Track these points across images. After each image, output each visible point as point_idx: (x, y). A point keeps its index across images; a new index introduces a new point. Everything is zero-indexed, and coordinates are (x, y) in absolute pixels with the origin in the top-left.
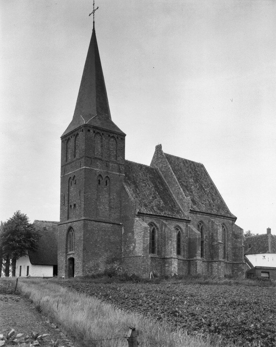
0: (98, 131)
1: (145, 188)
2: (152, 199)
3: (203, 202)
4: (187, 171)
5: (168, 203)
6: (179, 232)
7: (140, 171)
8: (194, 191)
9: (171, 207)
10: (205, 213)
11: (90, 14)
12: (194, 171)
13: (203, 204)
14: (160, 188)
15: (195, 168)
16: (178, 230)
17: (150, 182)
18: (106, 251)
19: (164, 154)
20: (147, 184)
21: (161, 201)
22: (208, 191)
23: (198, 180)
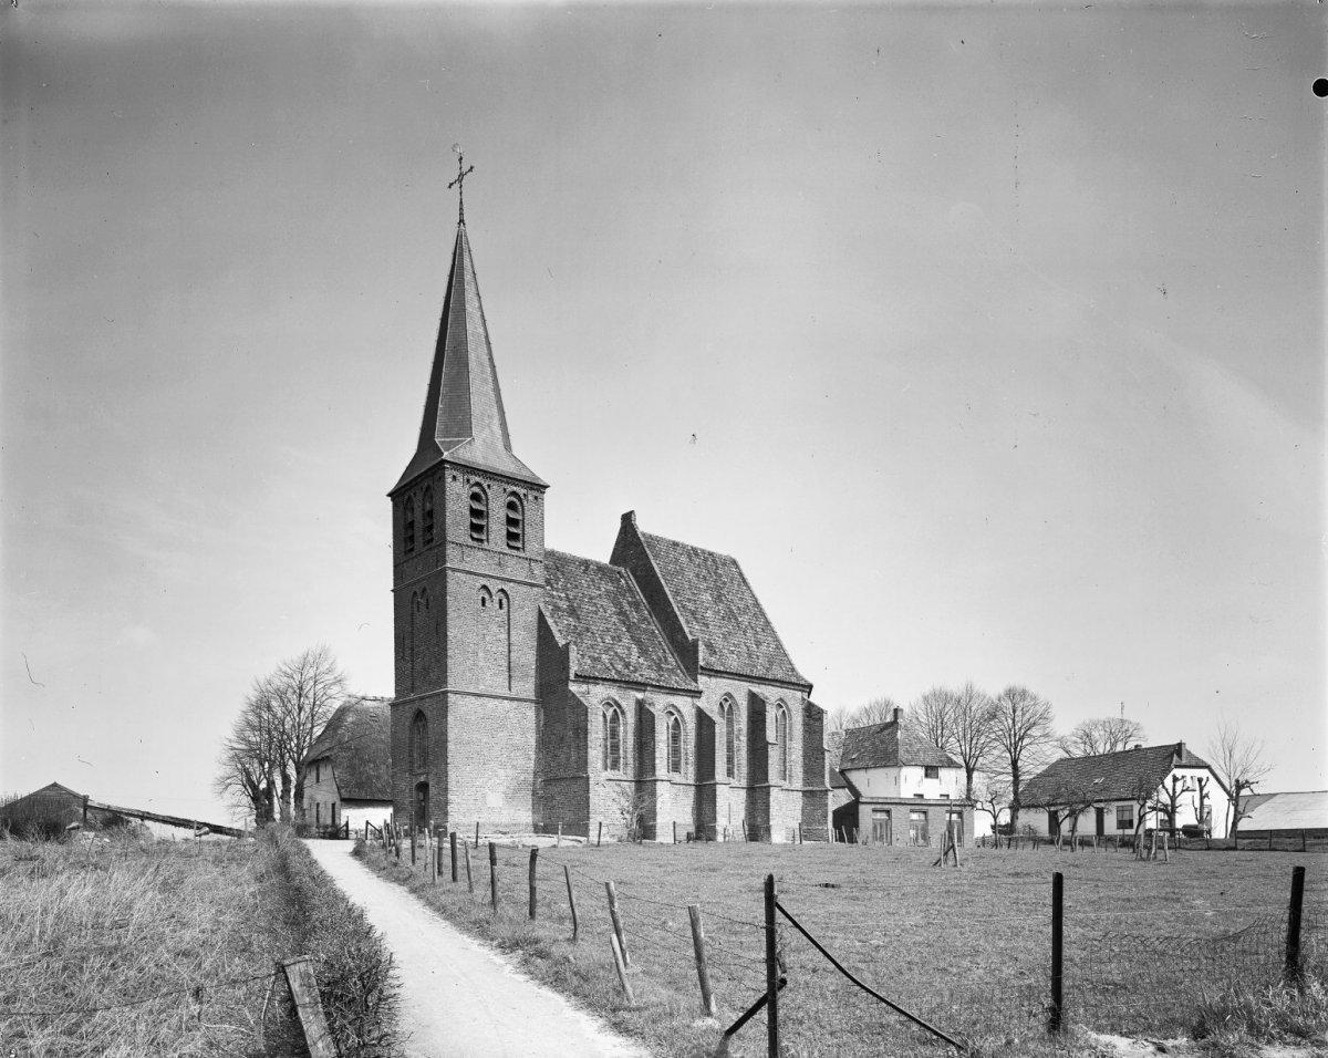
0: (477, 479)
4: (697, 576)
6: (676, 719)
10: (736, 674)
11: (451, 184)
17: (605, 602)
18: (503, 765)
19: (640, 536)
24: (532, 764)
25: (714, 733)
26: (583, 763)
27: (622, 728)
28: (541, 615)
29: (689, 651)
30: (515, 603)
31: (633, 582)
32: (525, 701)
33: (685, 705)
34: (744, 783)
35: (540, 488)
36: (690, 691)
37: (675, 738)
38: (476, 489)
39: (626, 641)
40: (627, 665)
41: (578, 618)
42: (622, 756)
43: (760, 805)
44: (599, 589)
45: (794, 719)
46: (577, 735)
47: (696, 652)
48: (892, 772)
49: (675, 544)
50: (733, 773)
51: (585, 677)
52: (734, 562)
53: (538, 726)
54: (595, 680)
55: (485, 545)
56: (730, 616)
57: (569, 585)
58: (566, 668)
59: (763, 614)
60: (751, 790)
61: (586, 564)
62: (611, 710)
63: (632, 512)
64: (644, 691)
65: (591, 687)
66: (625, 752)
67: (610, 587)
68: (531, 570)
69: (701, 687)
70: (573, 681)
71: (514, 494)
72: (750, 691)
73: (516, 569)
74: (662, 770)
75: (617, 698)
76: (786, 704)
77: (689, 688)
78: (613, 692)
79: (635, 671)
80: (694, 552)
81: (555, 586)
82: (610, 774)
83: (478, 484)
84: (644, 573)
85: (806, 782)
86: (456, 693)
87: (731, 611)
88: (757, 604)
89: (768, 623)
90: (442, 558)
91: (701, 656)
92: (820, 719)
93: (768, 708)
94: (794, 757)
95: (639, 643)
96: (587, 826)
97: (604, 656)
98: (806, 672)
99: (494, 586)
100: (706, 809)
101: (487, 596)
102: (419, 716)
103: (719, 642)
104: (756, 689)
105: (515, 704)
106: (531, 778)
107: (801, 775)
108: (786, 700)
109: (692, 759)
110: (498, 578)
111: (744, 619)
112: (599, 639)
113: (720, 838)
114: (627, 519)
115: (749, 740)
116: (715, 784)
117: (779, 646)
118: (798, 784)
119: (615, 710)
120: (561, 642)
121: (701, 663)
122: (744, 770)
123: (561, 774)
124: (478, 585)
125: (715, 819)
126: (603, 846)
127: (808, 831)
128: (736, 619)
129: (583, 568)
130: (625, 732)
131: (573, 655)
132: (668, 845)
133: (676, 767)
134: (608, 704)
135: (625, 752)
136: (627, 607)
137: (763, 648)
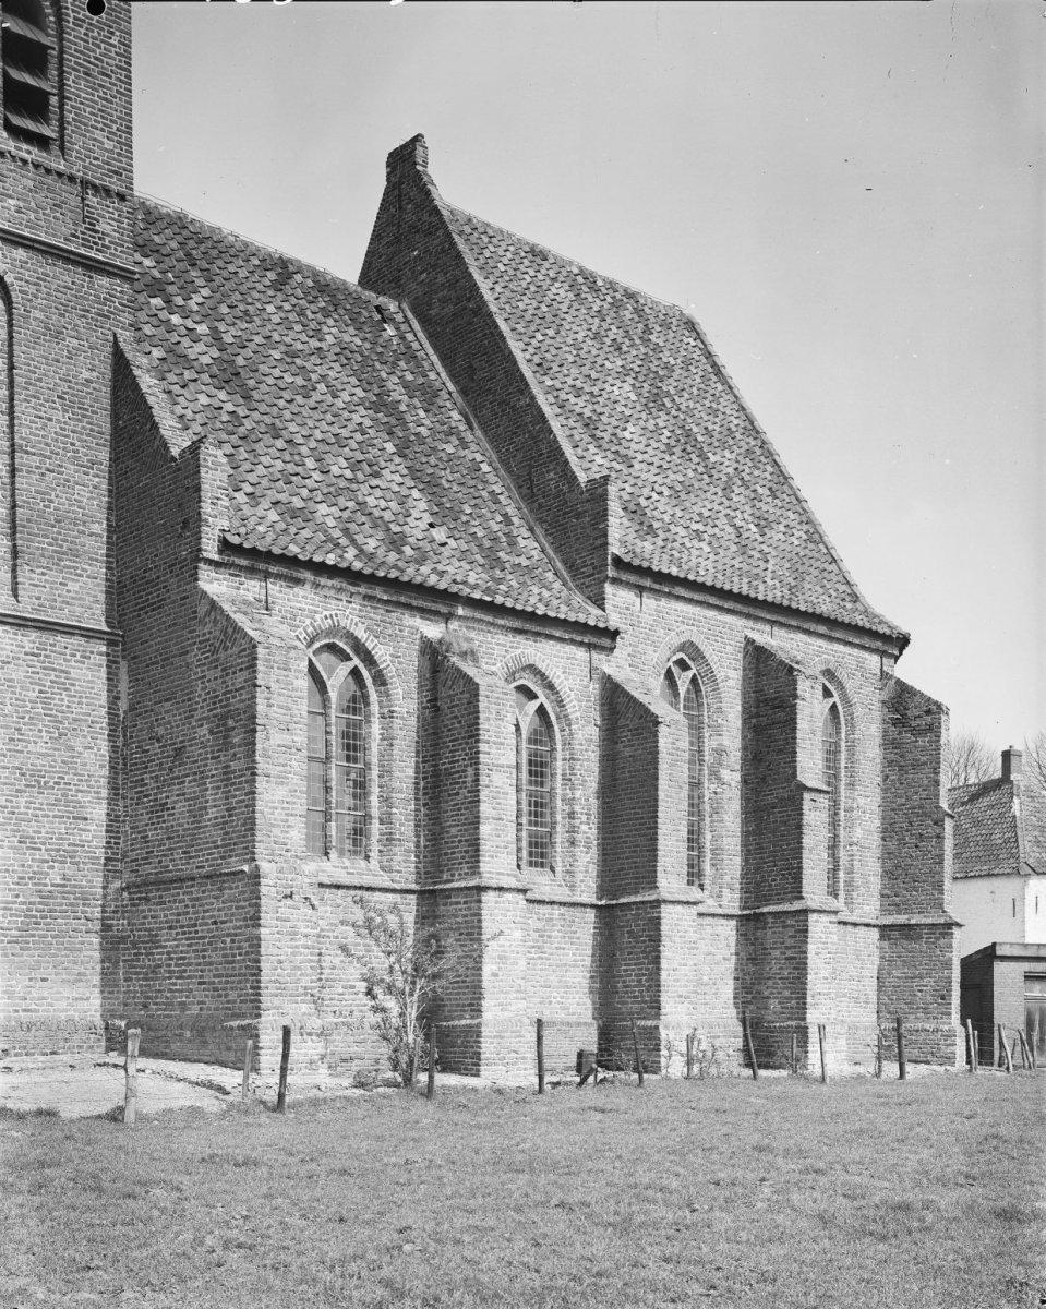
1: (299, 400)
2: (348, 473)
3: (695, 526)
5: (464, 518)
6: (541, 711)
7: (271, 293)
8: (640, 457)
9: (487, 543)
12: (638, 342)
13: (698, 535)
14: (408, 418)
15: (647, 330)
16: (535, 697)
20: (314, 377)
21: (416, 494)
22: (730, 470)
23: (668, 394)
24: (94, 835)
25: (654, 752)
26: (242, 828)
27: (376, 728)
28: (121, 368)
29: (578, 515)
31: (419, 338)
32: (67, 630)
33: (566, 665)
34: (731, 902)
36: (582, 628)
37: (538, 769)
39: (394, 476)
40: (396, 542)
41: (247, 397)
42: (375, 812)
43: (776, 963)
44: (318, 334)
45: (861, 727)
46: (222, 734)
47: (602, 515)
48: (1006, 887)
49: (538, 254)
50: (700, 874)
51: (253, 553)
52: (691, 326)
53: (112, 714)
54: (291, 567)
56: (686, 445)
57: (224, 309)
58: (191, 523)
59: (770, 454)
60: (751, 923)
61: (283, 270)
62: (343, 669)
63: (417, 139)
64: (448, 617)
65: (275, 588)
66: (386, 800)
67: (351, 337)
69: (614, 621)
70: (216, 564)
72: (749, 641)
74: (499, 856)
75: (361, 633)
76: (841, 686)
77: (582, 618)
78: (348, 613)
79: (421, 560)
80: (585, 283)
81: (179, 301)
82: (337, 868)
84: (449, 309)
85: (890, 901)
87: (688, 434)
88: (752, 429)
89: (782, 477)
91: (614, 534)
92: (933, 730)
93: (803, 687)
94: (858, 833)
95: (431, 487)
96: (252, 1033)
97: (323, 509)
98: (886, 605)
100: (629, 973)
103: (661, 509)
104: (765, 636)
105: (31, 639)
106: (93, 880)
107: (876, 883)
108: (842, 675)
109: (589, 830)
111: (724, 460)
112: (310, 463)
113: (675, 1067)
114: (405, 165)
115: (745, 781)
116: (657, 903)
117: (815, 536)
118: (869, 907)
119: (355, 673)
120: (178, 442)
121: (615, 548)
122: (733, 865)
123: (178, 865)
125: (655, 1007)
126: (292, 1107)
127: (896, 1044)
128: (703, 456)
129: (271, 275)
130: (388, 739)
131: (214, 476)
132: (518, 1098)
133: (539, 853)
134: (332, 648)
135: (386, 800)
136: (398, 394)
137: (776, 534)
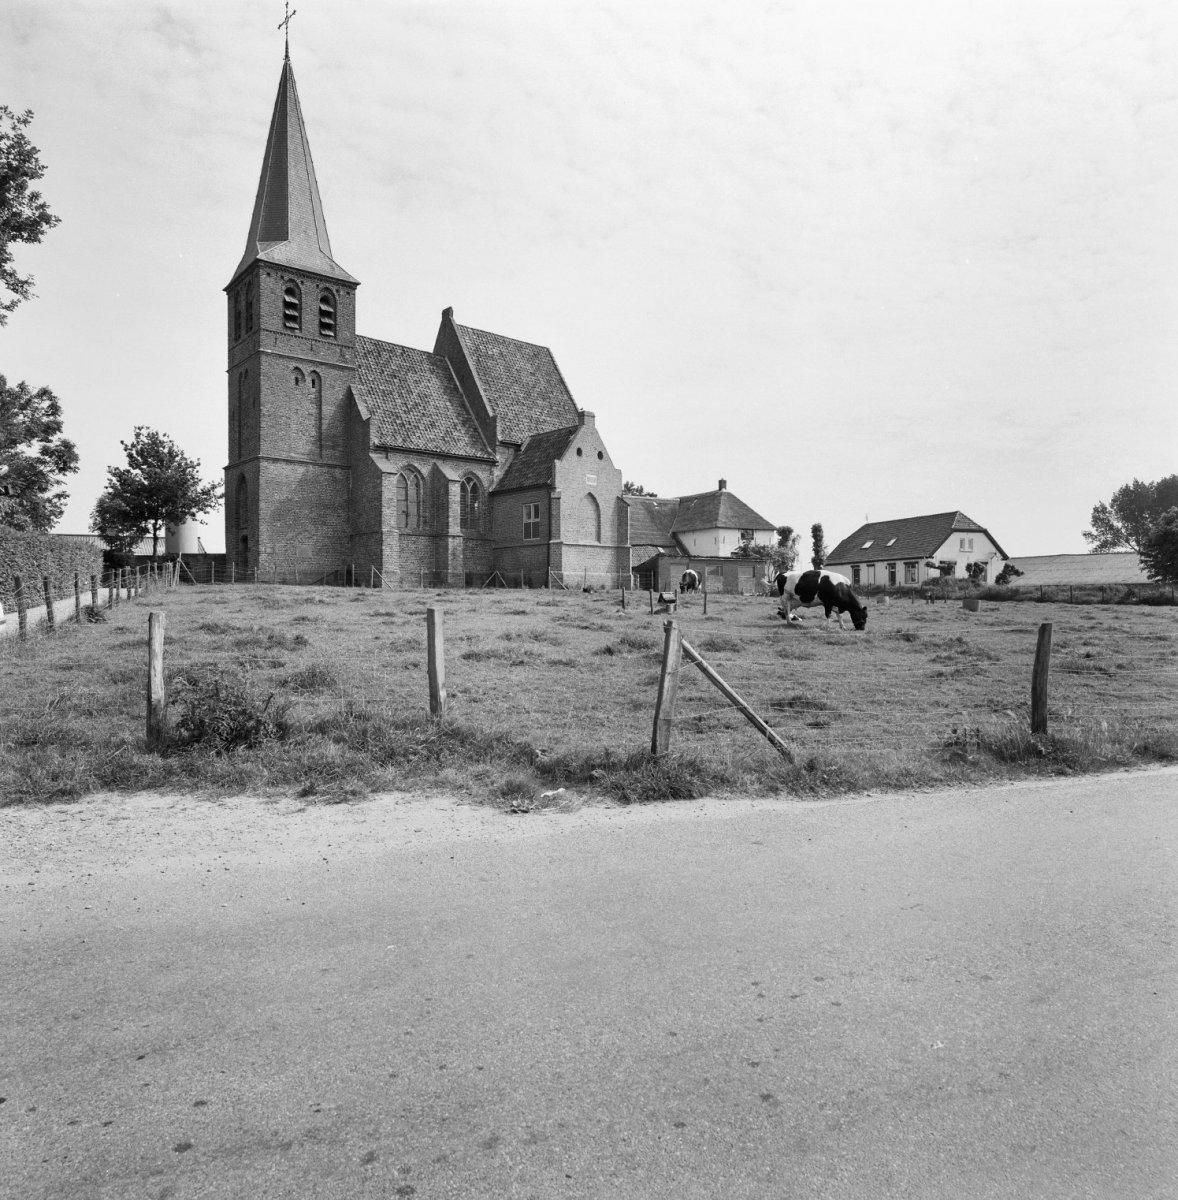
30: (326, 384)
35: (351, 286)
38: (290, 285)
55: (297, 332)
68: (342, 355)
71: (327, 289)
73: (326, 354)
83: (291, 280)
86: (268, 459)
90: (257, 343)
99: (307, 369)
101: (300, 377)
102: (242, 479)
110: (311, 361)
124: (291, 367)
